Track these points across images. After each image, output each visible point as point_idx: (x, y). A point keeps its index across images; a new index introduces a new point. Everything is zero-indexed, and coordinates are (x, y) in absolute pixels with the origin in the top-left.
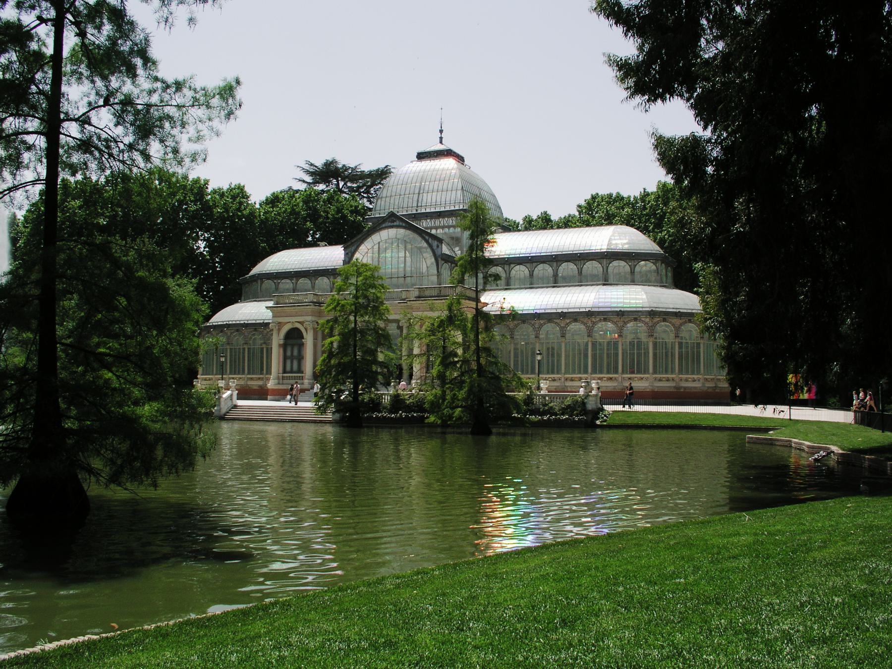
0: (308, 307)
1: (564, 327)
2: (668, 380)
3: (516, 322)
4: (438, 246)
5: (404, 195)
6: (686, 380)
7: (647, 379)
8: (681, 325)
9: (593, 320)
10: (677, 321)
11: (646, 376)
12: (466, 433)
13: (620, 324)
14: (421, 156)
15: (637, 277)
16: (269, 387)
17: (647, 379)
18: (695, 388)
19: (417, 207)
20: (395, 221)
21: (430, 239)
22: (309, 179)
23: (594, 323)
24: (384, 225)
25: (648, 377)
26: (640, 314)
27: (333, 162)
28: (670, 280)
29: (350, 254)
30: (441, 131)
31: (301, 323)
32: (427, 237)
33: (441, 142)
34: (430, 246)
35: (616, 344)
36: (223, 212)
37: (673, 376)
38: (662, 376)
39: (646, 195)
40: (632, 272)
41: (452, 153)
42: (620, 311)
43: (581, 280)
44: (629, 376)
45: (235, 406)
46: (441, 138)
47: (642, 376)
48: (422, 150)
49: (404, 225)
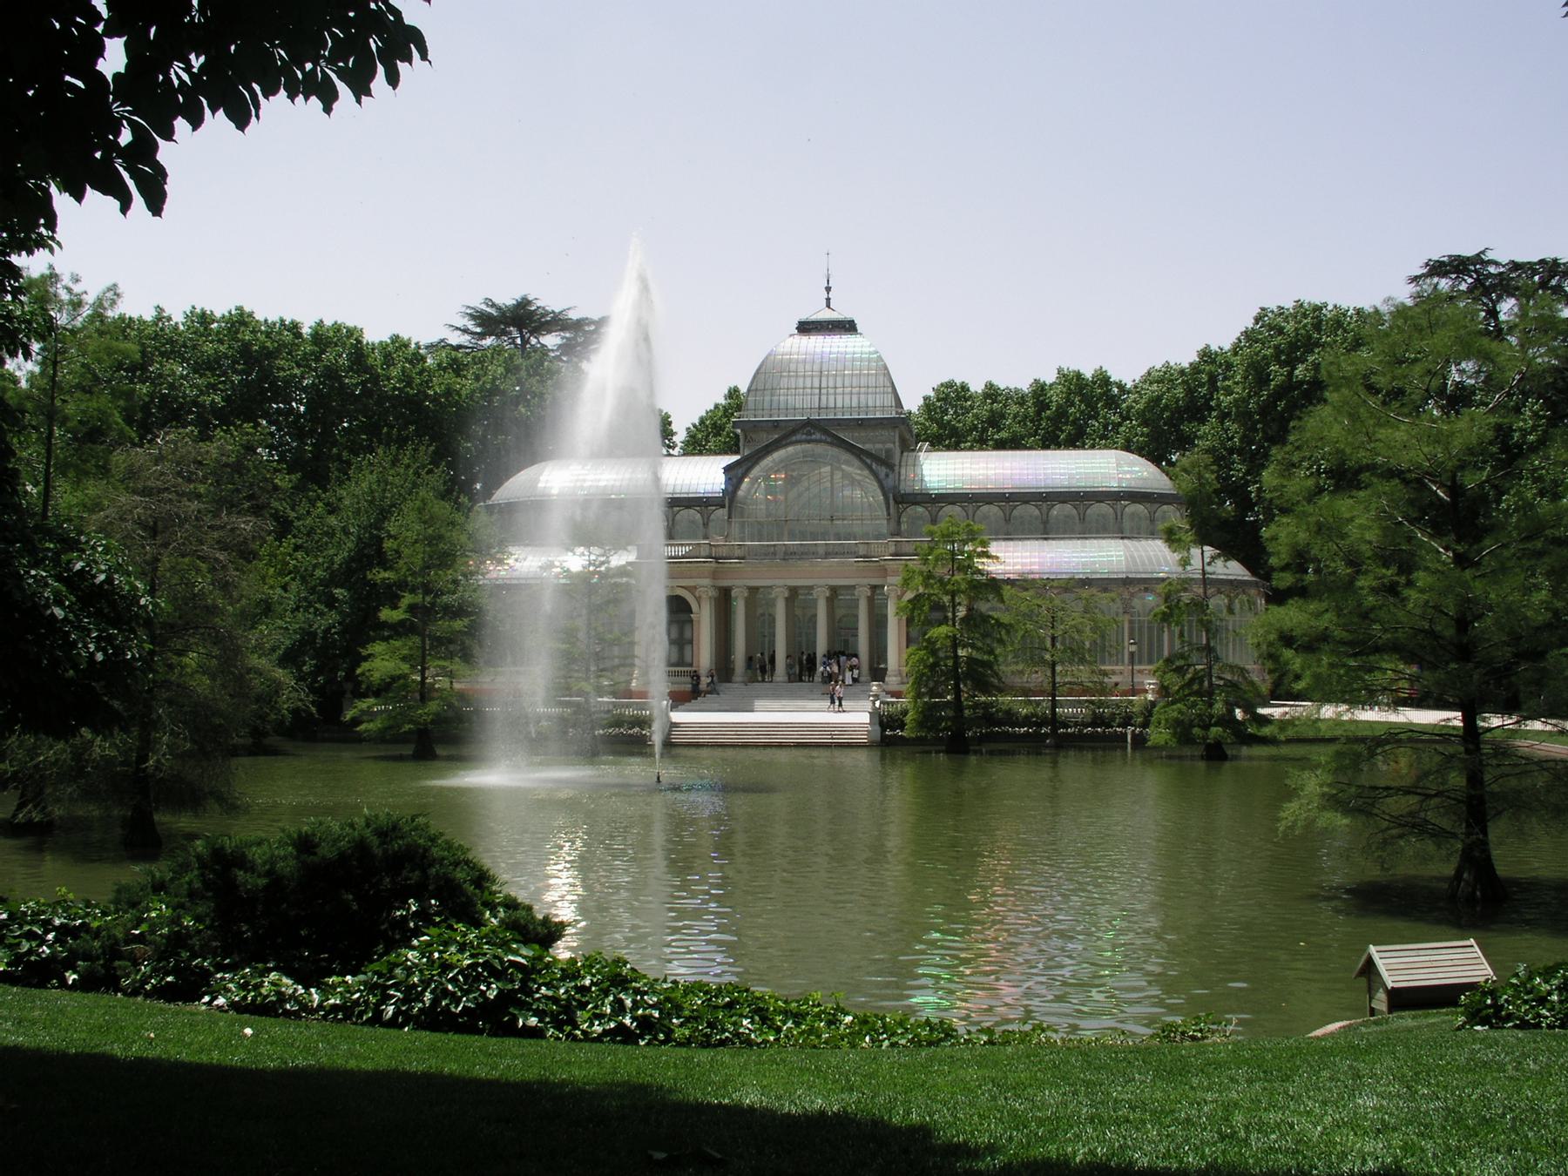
0: (707, 564)
4: (887, 475)
5: (851, 394)
12: (1192, 758)
14: (806, 328)
15: (1127, 524)
16: (633, 689)
19: (819, 408)
22: (471, 325)
23: (1132, 595)
24: (794, 438)
27: (529, 303)
29: (735, 480)
30: (828, 289)
31: (692, 589)
32: (869, 461)
33: (828, 306)
34: (875, 475)
36: (405, 387)
39: (1040, 389)
43: (1084, 529)
45: (676, 725)
46: (828, 300)
48: (804, 317)
49: (829, 440)
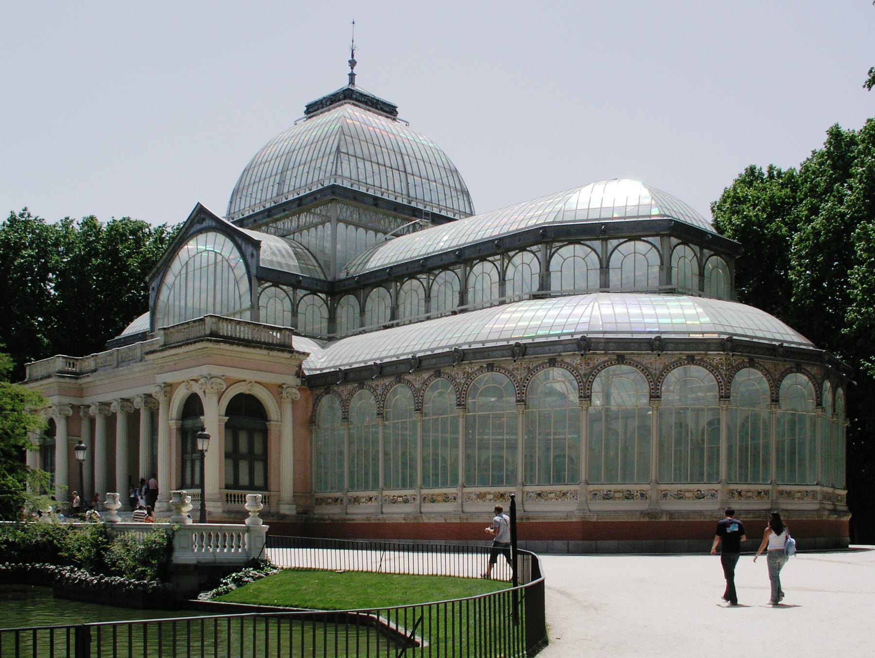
1: (419, 390)
2: (629, 496)
3: (350, 387)
4: (252, 255)
6: (680, 496)
7: (575, 495)
8: (667, 369)
9: (468, 369)
10: (650, 359)
11: (572, 488)
13: (520, 375)
14: (313, 109)
17: (575, 495)
18: (700, 513)
20: (203, 220)
21: (243, 244)
24: (192, 231)
25: (576, 492)
26: (559, 348)
28: (724, 285)
32: (239, 241)
35: (714, 424)
37: (645, 487)
38: (612, 487)
40: (604, 267)
41: (354, 96)
42: (518, 345)
44: (538, 489)
46: (352, 76)
47: (564, 488)
